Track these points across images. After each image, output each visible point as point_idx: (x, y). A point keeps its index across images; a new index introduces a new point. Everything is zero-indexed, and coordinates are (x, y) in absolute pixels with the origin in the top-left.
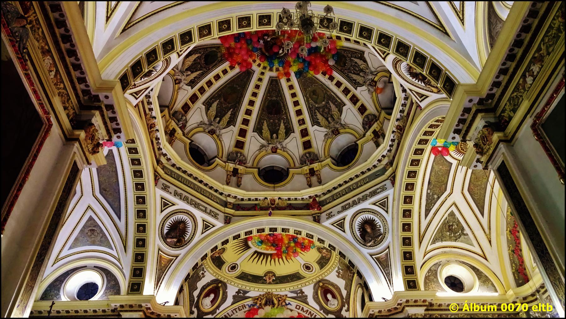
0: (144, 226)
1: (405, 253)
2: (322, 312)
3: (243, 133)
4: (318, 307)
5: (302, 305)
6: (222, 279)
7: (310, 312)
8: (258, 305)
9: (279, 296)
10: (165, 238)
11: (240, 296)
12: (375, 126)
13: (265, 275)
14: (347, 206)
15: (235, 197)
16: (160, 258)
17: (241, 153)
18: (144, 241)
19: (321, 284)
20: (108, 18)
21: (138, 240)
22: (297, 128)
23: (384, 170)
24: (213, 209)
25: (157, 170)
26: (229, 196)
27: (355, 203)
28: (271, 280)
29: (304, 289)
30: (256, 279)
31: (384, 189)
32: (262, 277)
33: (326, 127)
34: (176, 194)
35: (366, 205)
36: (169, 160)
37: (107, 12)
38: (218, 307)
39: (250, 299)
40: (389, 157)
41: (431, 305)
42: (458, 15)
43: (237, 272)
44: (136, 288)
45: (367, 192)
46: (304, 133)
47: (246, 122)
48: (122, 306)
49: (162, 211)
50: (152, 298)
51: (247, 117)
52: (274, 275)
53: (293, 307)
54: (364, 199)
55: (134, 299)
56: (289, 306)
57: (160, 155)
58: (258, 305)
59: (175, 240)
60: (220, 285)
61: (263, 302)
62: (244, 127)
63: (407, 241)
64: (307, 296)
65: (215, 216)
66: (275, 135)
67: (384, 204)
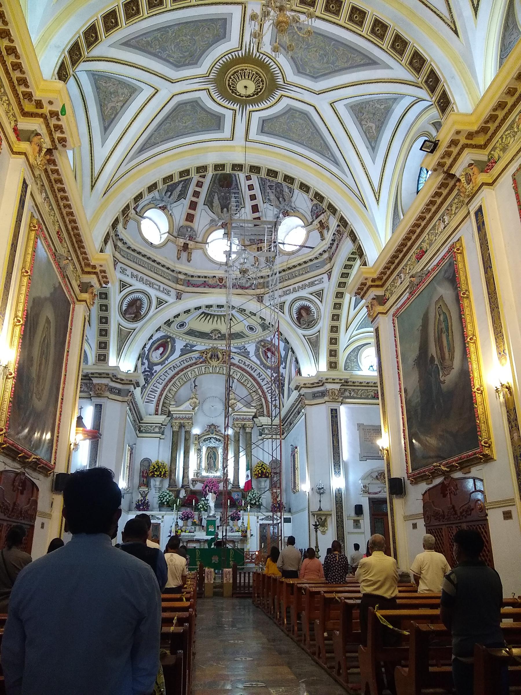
0: (106, 306)
1: (331, 339)
2: (262, 367)
3: (193, 206)
4: (258, 363)
5: (244, 359)
6: (171, 335)
7: (251, 366)
8: (204, 358)
9: (224, 351)
10: (124, 314)
11: (187, 350)
12: (322, 217)
13: (212, 333)
14: (288, 292)
15: (186, 274)
16: (120, 332)
17: (192, 229)
18: (106, 318)
19: (263, 344)
20: (92, 187)
21: (101, 318)
22: (249, 204)
23: (324, 263)
24: (166, 287)
25: (115, 256)
26: (180, 273)
27: (295, 290)
28: (217, 337)
29: (246, 346)
30: (202, 335)
31: (321, 281)
32: (208, 334)
33: (277, 207)
34: (132, 276)
35: (303, 293)
36: (125, 243)
37: (92, 181)
38: (167, 359)
39: (197, 352)
40: (329, 252)
41: (347, 382)
42: (375, 196)
43: (186, 329)
44: (102, 358)
45: (307, 282)
46: (255, 209)
47: (196, 194)
48: (92, 374)
49: (121, 292)
50: (117, 368)
51: (198, 189)
52: (220, 333)
53: (235, 361)
54: (303, 287)
55: (100, 368)
56: (232, 361)
57: (117, 240)
58: (204, 358)
59: (133, 316)
60: (169, 340)
61: (209, 355)
62: (194, 199)
63: (334, 329)
64: (249, 352)
65: (168, 293)
66: (225, 209)
67: (319, 294)
